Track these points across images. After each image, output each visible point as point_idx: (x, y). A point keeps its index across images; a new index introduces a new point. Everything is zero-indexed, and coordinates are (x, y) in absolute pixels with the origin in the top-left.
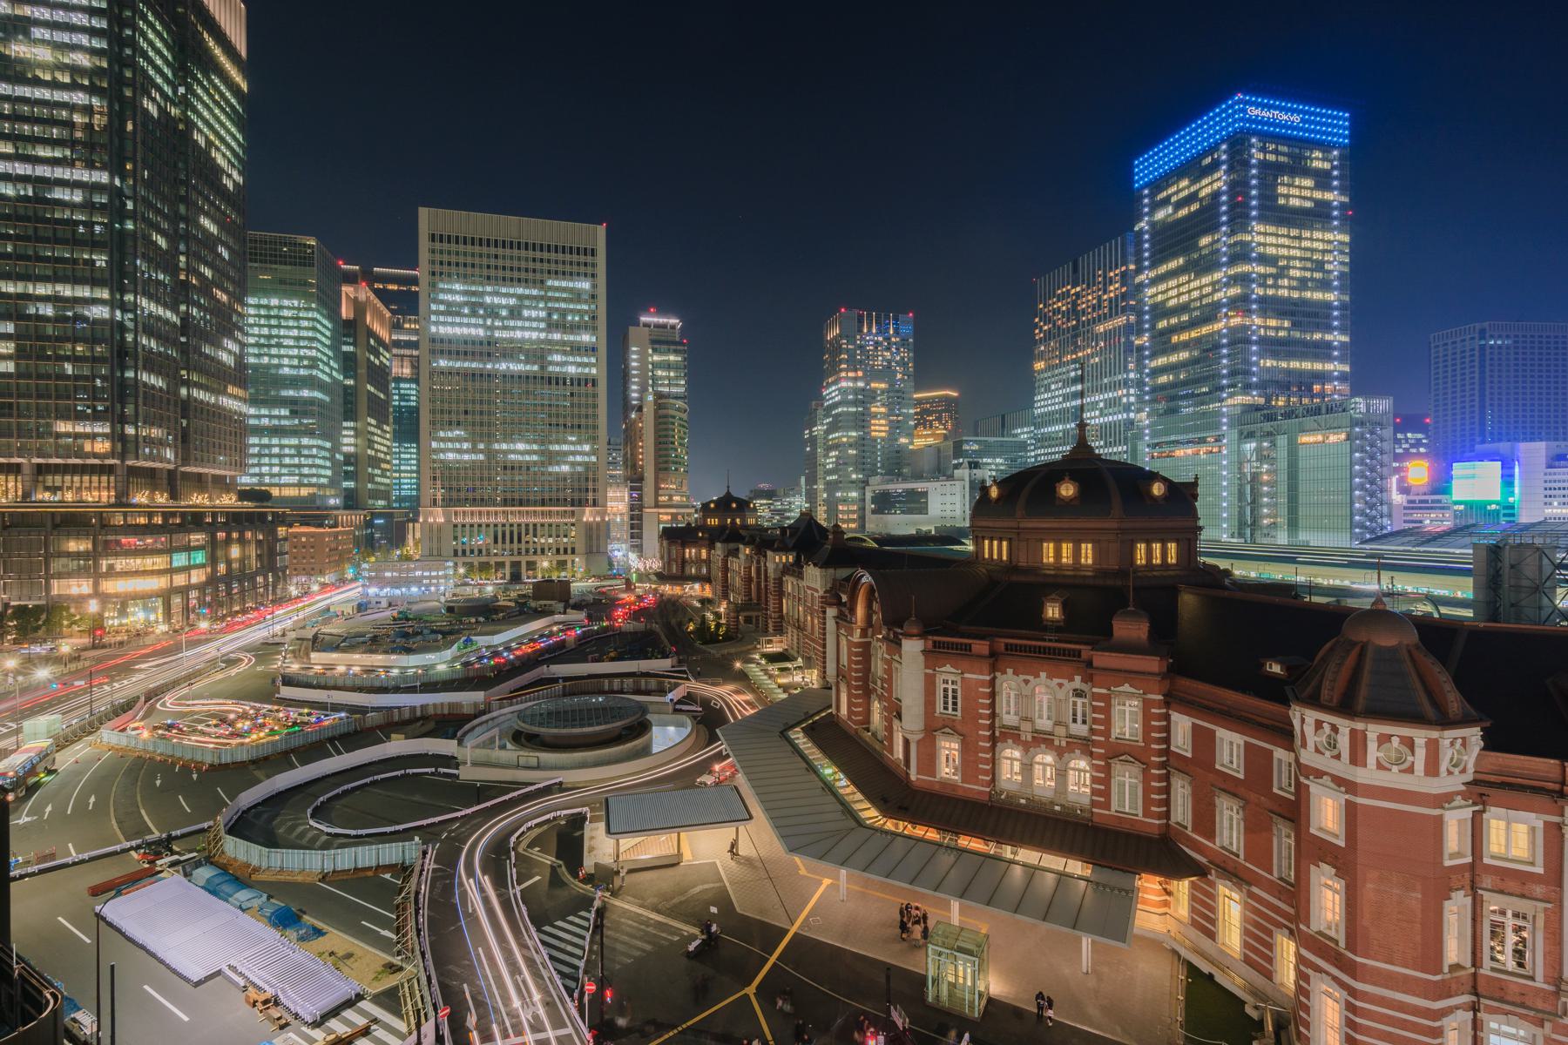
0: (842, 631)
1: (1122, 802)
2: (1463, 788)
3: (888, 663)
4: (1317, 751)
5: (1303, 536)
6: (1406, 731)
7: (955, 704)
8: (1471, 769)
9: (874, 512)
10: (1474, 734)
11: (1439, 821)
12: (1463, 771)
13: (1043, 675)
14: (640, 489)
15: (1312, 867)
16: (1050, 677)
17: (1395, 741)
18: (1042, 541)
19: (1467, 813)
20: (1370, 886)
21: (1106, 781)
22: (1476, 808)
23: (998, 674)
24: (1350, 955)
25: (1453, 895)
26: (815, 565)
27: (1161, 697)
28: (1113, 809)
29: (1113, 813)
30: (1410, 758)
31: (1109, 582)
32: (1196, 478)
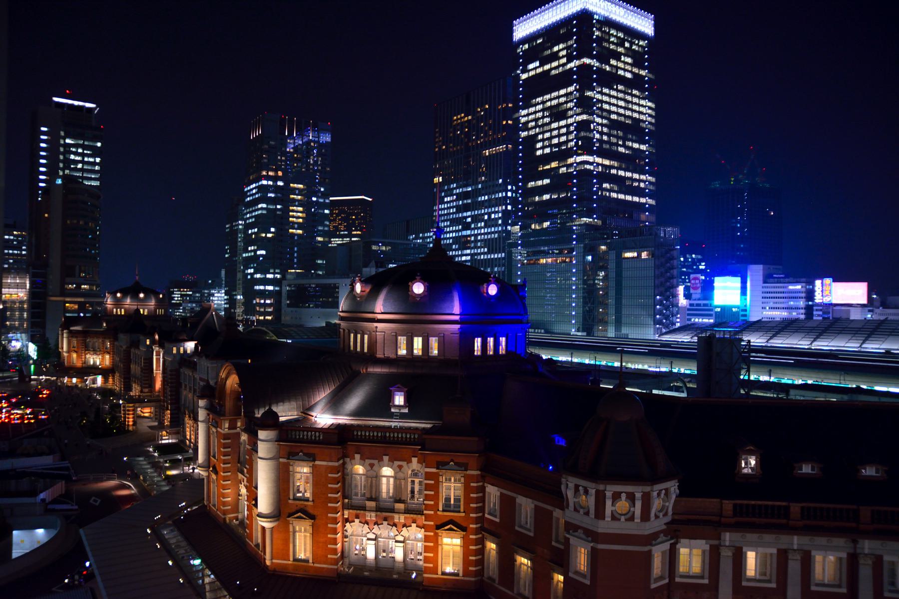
2: (664, 527)
5: (625, 330)
6: (630, 489)
9: (289, 306)
10: (673, 486)
11: (649, 556)
12: (666, 515)
13: (386, 458)
17: (624, 496)
19: (666, 546)
22: (672, 541)
23: (348, 460)
27: (478, 472)
28: (440, 573)
30: (632, 509)
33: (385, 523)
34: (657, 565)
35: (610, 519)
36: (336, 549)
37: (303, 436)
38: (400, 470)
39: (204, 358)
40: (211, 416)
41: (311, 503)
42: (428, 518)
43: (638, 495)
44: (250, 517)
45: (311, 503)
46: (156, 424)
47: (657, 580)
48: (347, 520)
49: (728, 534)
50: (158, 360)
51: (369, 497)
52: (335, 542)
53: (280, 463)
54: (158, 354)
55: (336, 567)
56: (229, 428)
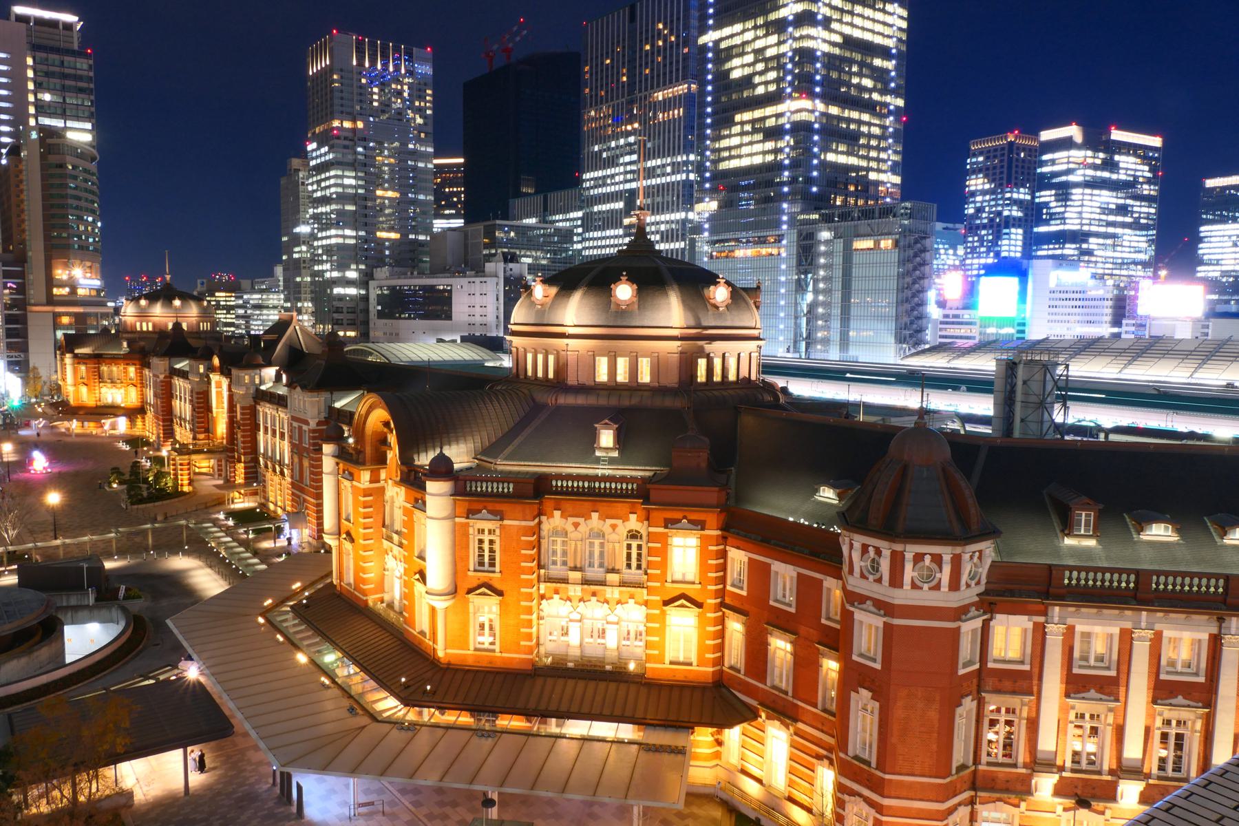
2: (977, 599)
3: (407, 512)
4: (863, 576)
6: (936, 549)
8: (984, 581)
9: (381, 315)
11: (957, 631)
12: (978, 583)
14: (21, 275)
15: (853, 694)
16: (603, 517)
17: (928, 559)
19: (977, 623)
20: (900, 704)
21: (661, 632)
22: (985, 617)
23: (544, 518)
25: (963, 701)
26: (304, 388)
27: (719, 532)
28: (667, 661)
31: (668, 402)
33: (594, 599)
34: (967, 649)
35: (909, 587)
36: (530, 635)
37: (503, 488)
39: (298, 389)
40: (341, 465)
41: (498, 575)
42: (650, 591)
43: (947, 558)
44: (408, 596)
45: (498, 575)
46: (221, 482)
47: (965, 666)
48: (542, 597)
49: (1057, 609)
50: (219, 394)
51: (572, 565)
52: (529, 624)
53: (455, 524)
54: (219, 385)
55: (530, 657)
56: (371, 482)
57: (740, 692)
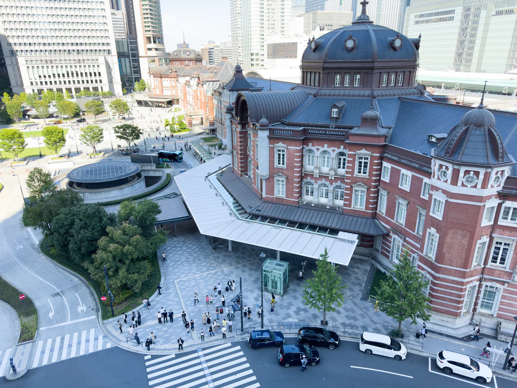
0: (234, 126)
1: (356, 204)
4: (438, 179)
7: (283, 161)
12: (499, 185)
15: (428, 230)
16: (328, 147)
17: (472, 173)
18: (336, 73)
20: (449, 236)
23: (305, 146)
24: (436, 264)
29: (352, 208)
30: (476, 181)
32: (420, 37)
38: (334, 152)
56: (242, 129)
57: (383, 222)
